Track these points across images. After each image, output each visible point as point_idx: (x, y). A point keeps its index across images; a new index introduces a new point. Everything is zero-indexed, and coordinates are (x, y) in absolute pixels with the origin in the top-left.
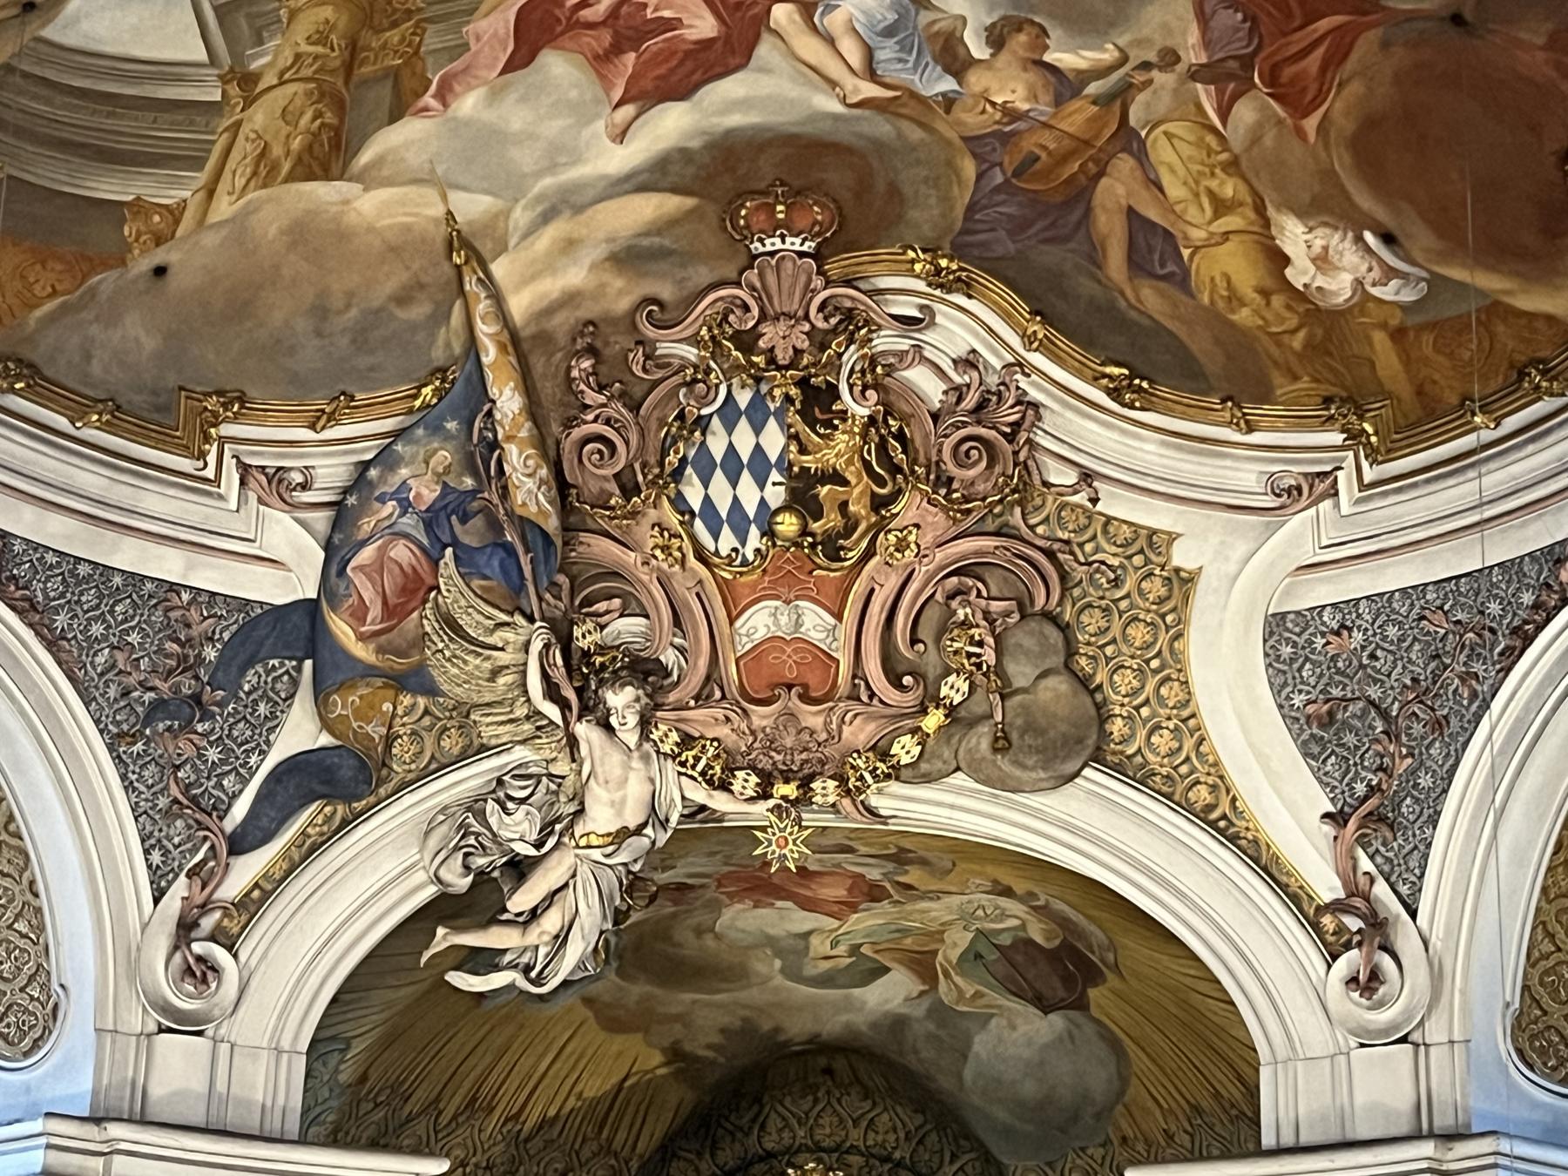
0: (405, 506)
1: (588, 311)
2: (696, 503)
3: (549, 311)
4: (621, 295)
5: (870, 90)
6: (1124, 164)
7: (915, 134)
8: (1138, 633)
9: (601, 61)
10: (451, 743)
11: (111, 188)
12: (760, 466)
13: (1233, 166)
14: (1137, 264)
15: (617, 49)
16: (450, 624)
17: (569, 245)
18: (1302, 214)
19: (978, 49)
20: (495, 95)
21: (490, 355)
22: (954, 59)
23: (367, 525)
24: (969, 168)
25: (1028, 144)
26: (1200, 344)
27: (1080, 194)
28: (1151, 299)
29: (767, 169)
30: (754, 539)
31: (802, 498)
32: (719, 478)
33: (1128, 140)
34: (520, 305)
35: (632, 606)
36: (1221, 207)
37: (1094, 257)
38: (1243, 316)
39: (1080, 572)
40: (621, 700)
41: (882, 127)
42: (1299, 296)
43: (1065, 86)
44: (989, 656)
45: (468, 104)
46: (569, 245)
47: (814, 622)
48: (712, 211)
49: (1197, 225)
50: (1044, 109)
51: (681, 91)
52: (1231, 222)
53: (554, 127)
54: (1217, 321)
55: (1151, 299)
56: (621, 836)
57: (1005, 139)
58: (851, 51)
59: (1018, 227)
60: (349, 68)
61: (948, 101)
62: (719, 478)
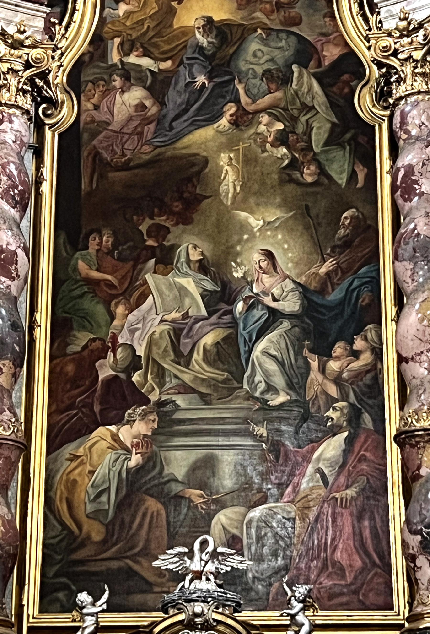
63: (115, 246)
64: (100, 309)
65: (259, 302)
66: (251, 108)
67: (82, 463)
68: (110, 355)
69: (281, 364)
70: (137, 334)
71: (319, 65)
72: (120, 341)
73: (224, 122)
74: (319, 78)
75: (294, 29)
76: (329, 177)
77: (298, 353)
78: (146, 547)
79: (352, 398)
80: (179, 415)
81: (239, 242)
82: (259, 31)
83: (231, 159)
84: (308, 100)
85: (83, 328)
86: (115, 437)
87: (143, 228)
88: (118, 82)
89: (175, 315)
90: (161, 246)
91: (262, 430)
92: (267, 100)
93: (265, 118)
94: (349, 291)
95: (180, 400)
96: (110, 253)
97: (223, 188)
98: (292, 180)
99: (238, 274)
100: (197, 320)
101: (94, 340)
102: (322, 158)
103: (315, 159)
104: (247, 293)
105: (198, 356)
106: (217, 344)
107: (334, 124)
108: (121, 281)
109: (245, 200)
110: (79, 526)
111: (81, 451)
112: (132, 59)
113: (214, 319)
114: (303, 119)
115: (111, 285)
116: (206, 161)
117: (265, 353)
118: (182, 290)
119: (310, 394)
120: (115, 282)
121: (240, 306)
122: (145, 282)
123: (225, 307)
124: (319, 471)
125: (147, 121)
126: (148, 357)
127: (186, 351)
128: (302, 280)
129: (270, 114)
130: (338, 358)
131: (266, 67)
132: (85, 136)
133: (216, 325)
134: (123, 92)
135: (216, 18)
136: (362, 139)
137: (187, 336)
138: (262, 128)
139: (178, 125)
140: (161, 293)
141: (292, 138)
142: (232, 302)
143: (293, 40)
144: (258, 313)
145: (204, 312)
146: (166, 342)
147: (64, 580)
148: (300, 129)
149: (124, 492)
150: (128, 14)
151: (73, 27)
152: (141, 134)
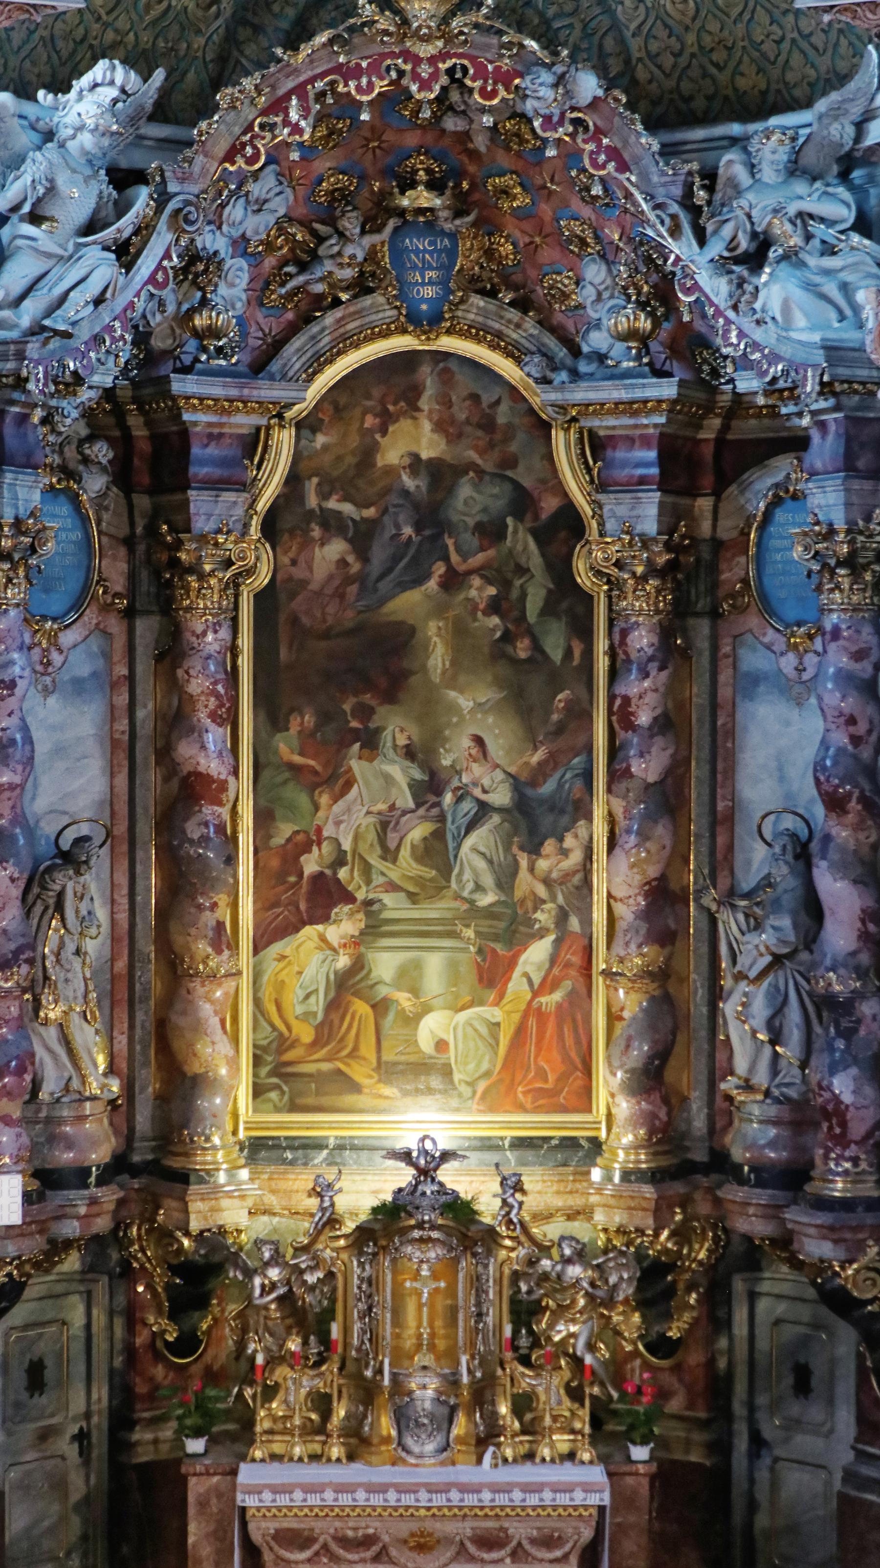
63: (318, 727)
64: (303, 800)
65: (468, 793)
66: (462, 568)
67: (289, 963)
68: (315, 849)
69: (490, 862)
70: (342, 826)
71: (536, 517)
72: (325, 834)
73: (432, 584)
74: (536, 533)
75: (509, 473)
76: (543, 652)
77: (507, 848)
78: (356, 1048)
79: (560, 899)
80: (386, 915)
81: (449, 724)
82: (471, 474)
83: (439, 628)
84: (523, 561)
85: (287, 819)
86: (323, 938)
87: (347, 707)
88: (316, 532)
89: (382, 807)
90: (366, 728)
91: (470, 933)
92: (479, 559)
93: (476, 581)
94: (560, 785)
95: (388, 899)
96: (312, 734)
97: (431, 662)
98: (504, 655)
99: (446, 762)
100: (405, 813)
101: (297, 832)
102: (537, 630)
103: (530, 632)
104: (455, 783)
105: (405, 853)
106: (425, 839)
107: (550, 591)
108: (326, 766)
109: (454, 678)
110: (289, 1028)
111: (287, 952)
112: (332, 504)
113: (421, 811)
114: (518, 583)
115: (316, 773)
116: (412, 631)
117: (475, 850)
118: (388, 779)
119: (518, 894)
120: (318, 768)
121: (448, 798)
122: (350, 769)
123: (433, 799)
124: (526, 975)
125: (348, 580)
126: (354, 851)
127: (392, 845)
128: (512, 770)
129: (482, 577)
130: (547, 856)
131: (478, 518)
132: (283, 597)
133: (424, 818)
134: (322, 545)
135: (425, 455)
136: (580, 610)
137: (395, 829)
138: (473, 593)
139: (384, 586)
140: (367, 783)
141: (505, 605)
142: (439, 792)
143: (508, 487)
144: (468, 806)
145: (411, 804)
146: (372, 836)
147: (274, 1080)
148: (515, 594)
149: (332, 994)
150: (325, 448)
151: (267, 466)
152: (342, 596)
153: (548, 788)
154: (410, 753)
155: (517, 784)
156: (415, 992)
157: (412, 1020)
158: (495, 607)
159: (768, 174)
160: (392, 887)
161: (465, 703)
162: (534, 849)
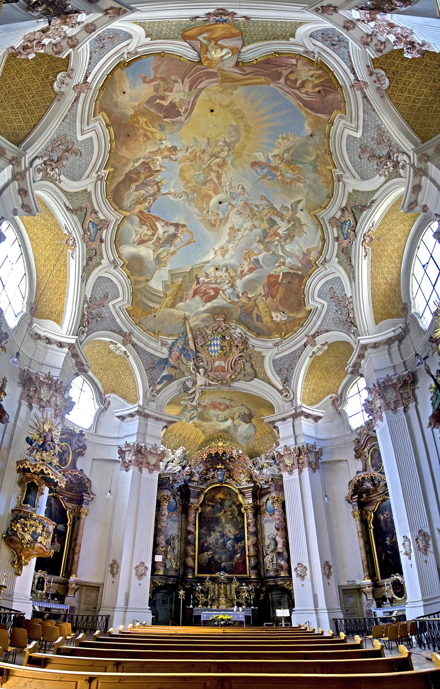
0: (178, 348)
1: (199, 327)
2: (210, 349)
3: (195, 326)
4: (202, 325)
5: (229, 301)
6: (256, 308)
7: (234, 306)
8: (259, 363)
9: (202, 297)
10: (182, 376)
11: (152, 305)
12: (217, 345)
13: (267, 307)
14: (257, 320)
15: (203, 296)
16: (182, 362)
17: (197, 319)
18: (274, 312)
19: (241, 295)
20: (191, 300)
21: (188, 331)
22: (238, 297)
23: (174, 349)
24: (240, 310)
25: (246, 307)
26: (264, 329)
27: (251, 312)
28: (259, 324)
29: (218, 311)
30: (217, 353)
31: (222, 349)
32: (212, 347)
33: (256, 305)
34: (192, 325)
35: (202, 361)
36: (266, 312)
37: (253, 320)
38: (269, 325)
39: (252, 357)
40: (201, 370)
41: (231, 305)
42: (274, 321)
43: (250, 299)
44: (243, 366)
45: (188, 301)
46: (197, 319)
47: (223, 363)
48: (212, 316)
49: (263, 314)
50: (247, 302)
51: (210, 301)
52: (267, 314)
53: (196, 305)
54: (266, 325)
55: (259, 324)
56: (201, 386)
57: (244, 306)
58: (228, 296)
59: (245, 317)
60: (176, 295)
61: (238, 302)
62: (212, 347)
153: (239, 536)
154: (220, 532)
155: (234, 535)
156: (221, 560)
157: (221, 563)
158: (231, 515)
159: (263, 459)
160: (218, 548)
161: (227, 526)
162: (237, 543)
